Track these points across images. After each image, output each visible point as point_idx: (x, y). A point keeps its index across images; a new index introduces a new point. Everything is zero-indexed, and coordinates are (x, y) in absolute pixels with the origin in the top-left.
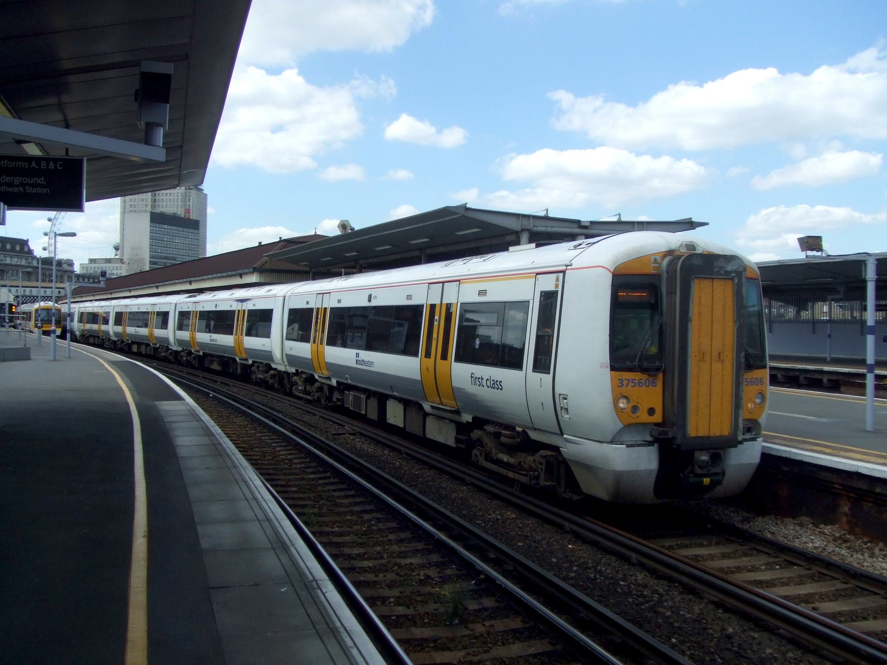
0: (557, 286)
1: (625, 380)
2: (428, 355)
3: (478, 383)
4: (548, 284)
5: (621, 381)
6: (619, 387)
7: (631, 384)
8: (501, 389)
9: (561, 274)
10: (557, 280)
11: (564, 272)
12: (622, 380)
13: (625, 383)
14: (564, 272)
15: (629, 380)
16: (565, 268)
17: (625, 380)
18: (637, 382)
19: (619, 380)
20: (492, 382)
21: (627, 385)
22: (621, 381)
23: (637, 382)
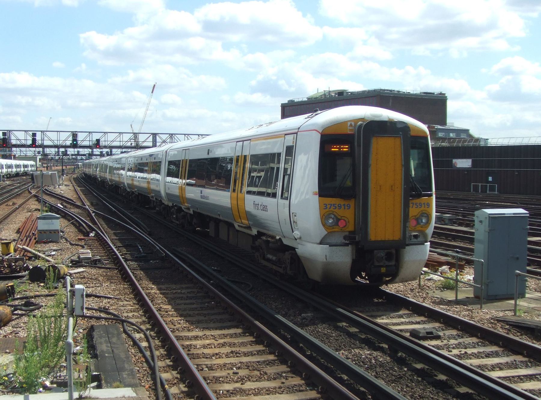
0: (293, 143)
1: (329, 204)
2: (234, 190)
3: (257, 208)
4: (289, 140)
5: (325, 205)
6: (324, 209)
7: (332, 207)
8: (267, 211)
9: (296, 134)
10: (294, 138)
11: (297, 133)
12: (326, 205)
13: (328, 206)
14: (297, 133)
15: (331, 205)
16: (297, 131)
17: (329, 204)
18: (337, 206)
19: (325, 204)
20: (263, 207)
21: (330, 208)
22: (325, 205)
23: (337, 206)
